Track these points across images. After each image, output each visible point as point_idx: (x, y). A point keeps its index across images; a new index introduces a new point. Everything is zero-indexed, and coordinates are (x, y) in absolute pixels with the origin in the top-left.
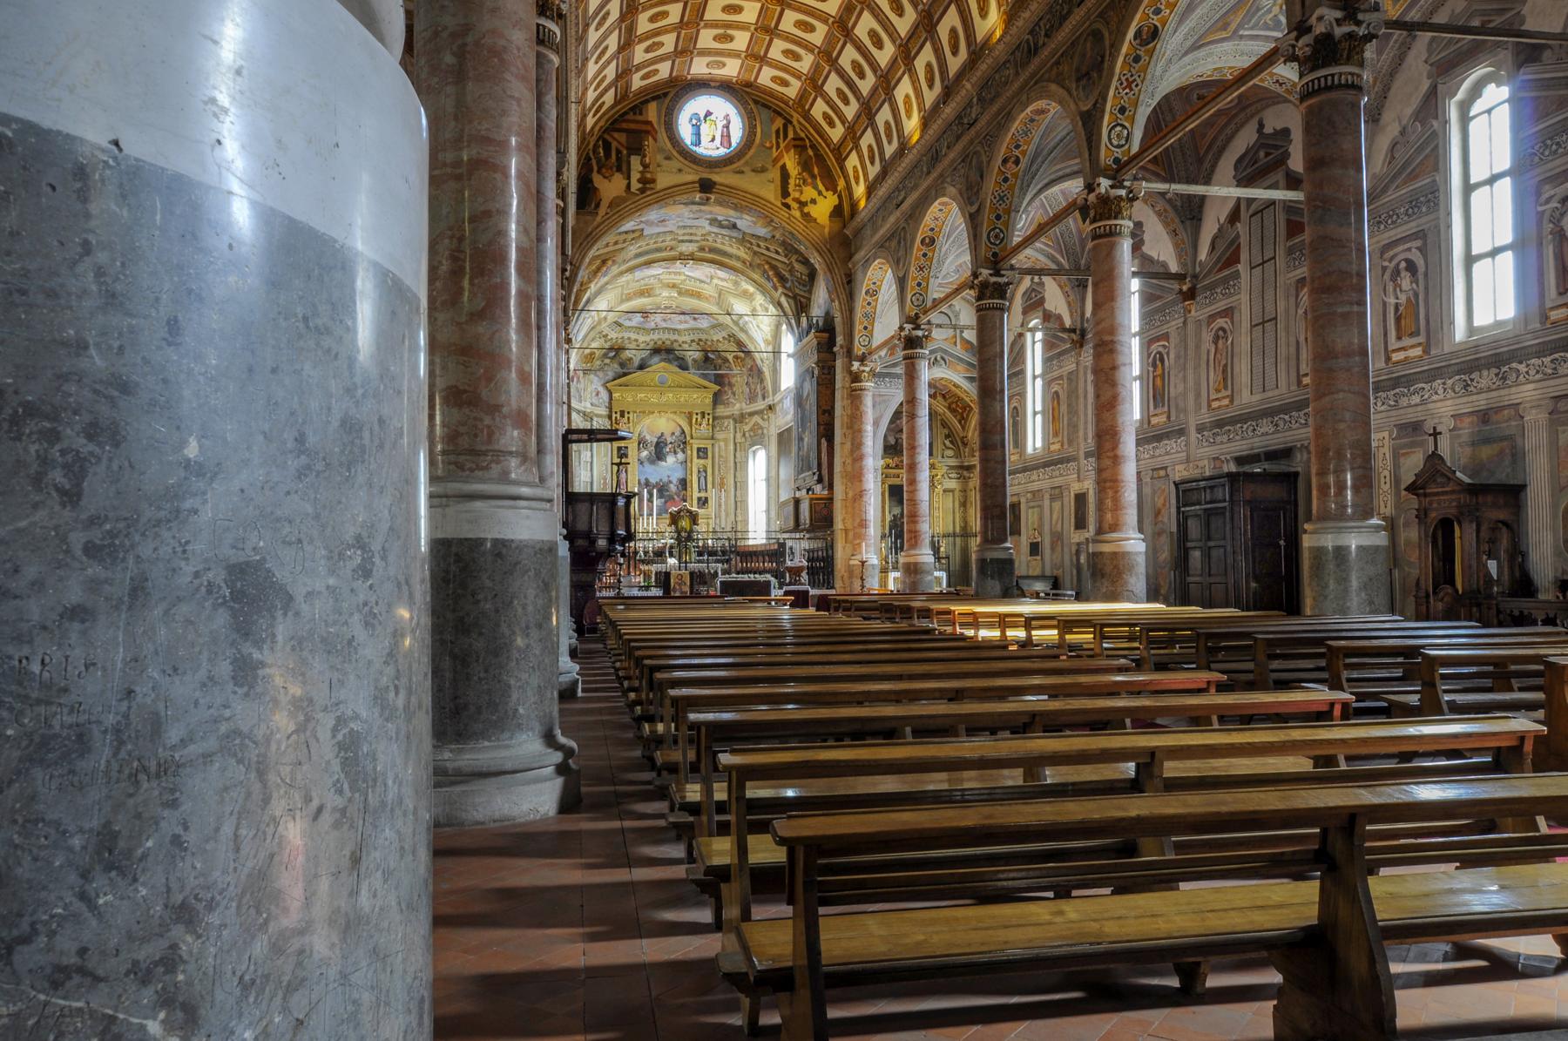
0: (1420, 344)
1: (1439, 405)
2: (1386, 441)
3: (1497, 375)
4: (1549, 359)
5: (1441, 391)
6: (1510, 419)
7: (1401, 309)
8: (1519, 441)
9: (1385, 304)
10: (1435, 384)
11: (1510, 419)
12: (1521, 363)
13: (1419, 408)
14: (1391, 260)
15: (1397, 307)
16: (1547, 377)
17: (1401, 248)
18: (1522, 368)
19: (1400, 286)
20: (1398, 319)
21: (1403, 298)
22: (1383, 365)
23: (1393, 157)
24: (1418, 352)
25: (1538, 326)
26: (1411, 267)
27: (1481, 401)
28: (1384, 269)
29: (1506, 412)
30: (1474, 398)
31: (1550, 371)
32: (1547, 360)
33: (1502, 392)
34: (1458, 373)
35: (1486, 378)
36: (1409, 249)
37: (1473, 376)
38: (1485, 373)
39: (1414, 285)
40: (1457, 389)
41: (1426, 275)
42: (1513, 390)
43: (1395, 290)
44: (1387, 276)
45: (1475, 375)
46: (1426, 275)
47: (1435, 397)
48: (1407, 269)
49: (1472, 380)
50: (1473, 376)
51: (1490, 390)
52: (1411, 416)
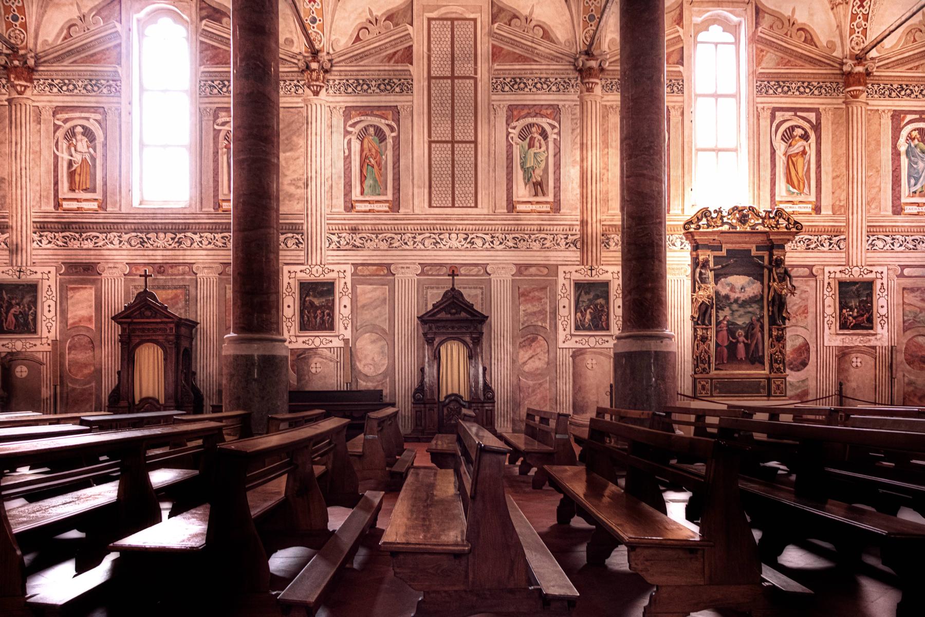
0: (96, 200)
1: (114, 252)
2: (52, 275)
3: (173, 239)
4: (220, 235)
5: (116, 241)
6: (184, 274)
7: (75, 166)
8: (192, 290)
9: (56, 157)
10: (111, 235)
11: (184, 274)
12: (195, 233)
13: (92, 252)
14: (66, 121)
15: (70, 164)
16: (217, 248)
17: (77, 115)
18: (196, 237)
19: (75, 147)
20: (71, 175)
21: (78, 158)
22: (51, 208)
23: (69, 35)
24: (94, 206)
25: (212, 210)
26: (87, 132)
27: (159, 257)
28: (57, 128)
29: (181, 268)
30: (150, 253)
31: (221, 245)
32: (218, 236)
33: (178, 253)
34: (135, 231)
35: (163, 240)
36: (88, 119)
37: (149, 236)
38: (162, 235)
39: (91, 150)
40: (133, 243)
41: (105, 145)
42: (188, 252)
43: (69, 148)
44: (60, 133)
45: (152, 235)
46: (105, 145)
47: (110, 246)
48: (83, 134)
49: (149, 239)
50: (149, 236)
51: (165, 249)
52: (83, 257)
